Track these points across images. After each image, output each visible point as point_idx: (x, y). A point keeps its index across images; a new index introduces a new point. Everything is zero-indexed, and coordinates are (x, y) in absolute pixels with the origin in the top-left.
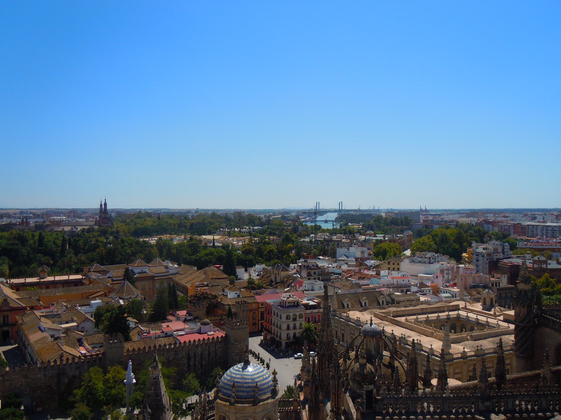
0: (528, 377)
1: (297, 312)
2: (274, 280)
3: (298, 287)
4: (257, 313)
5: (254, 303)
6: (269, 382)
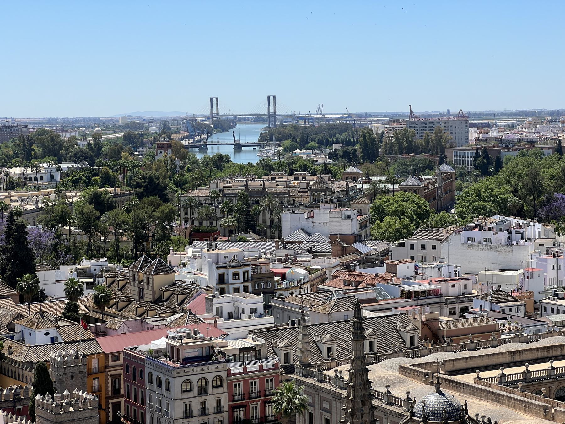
1: (210, 372)
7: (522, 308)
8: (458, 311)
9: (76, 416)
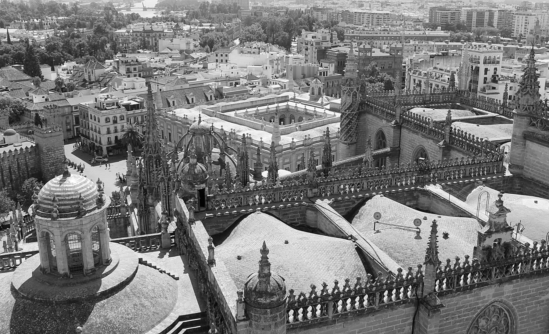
0: (352, 162)
2: (87, 80)
3: (116, 85)
4: (70, 118)
5: (66, 106)
6: (94, 192)
7: (261, 83)
8: (234, 83)
9: (52, 134)
